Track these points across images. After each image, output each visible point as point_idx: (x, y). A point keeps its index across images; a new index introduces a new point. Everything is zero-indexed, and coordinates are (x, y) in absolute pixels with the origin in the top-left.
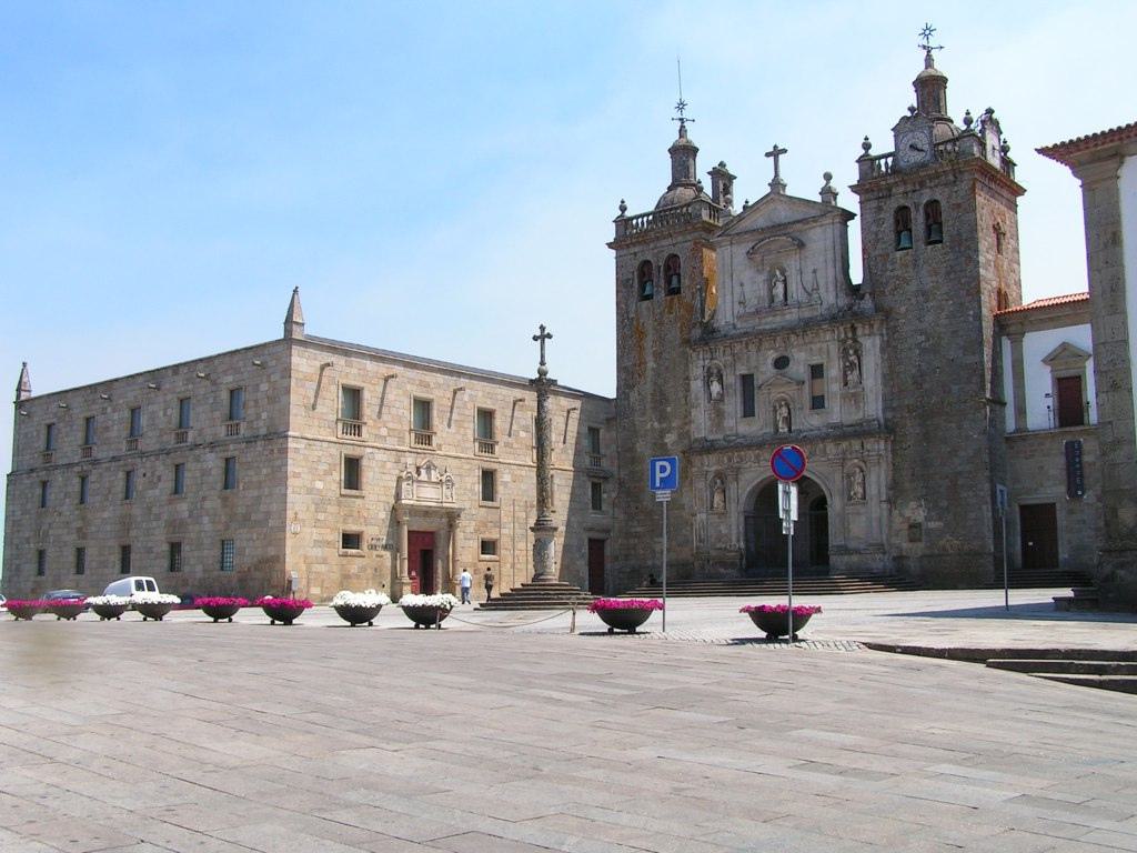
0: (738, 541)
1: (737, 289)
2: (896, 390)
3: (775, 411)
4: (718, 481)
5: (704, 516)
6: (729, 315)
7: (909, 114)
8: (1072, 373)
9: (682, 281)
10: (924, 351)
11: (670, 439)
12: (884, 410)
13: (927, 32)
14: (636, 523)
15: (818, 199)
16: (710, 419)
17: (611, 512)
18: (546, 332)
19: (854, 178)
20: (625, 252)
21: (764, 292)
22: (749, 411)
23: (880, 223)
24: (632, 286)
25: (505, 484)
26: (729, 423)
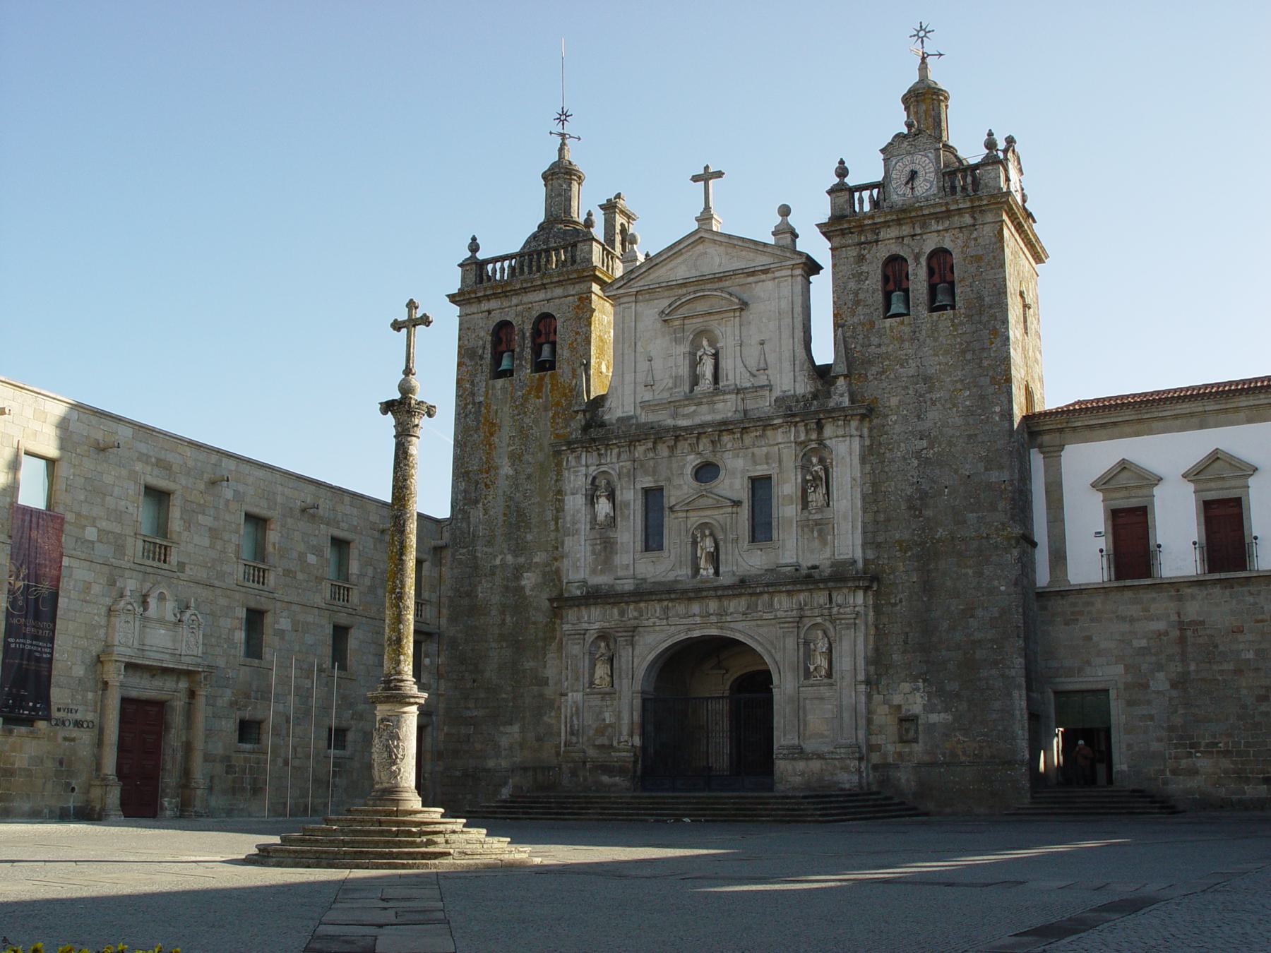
0: (631, 735)
1: (643, 366)
2: (882, 517)
3: (695, 543)
4: (603, 644)
5: (579, 696)
6: (629, 400)
7: (905, 131)
8: (1134, 503)
9: (559, 350)
11: (529, 580)
12: (865, 545)
13: (922, 34)
14: (471, 705)
15: (771, 240)
16: (593, 552)
17: (435, 686)
18: (418, 314)
19: (824, 214)
20: (474, 308)
21: (684, 370)
22: (652, 540)
23: (859, 277)
24: (481, 358)
25: (281, 634)
26: (622, 559)
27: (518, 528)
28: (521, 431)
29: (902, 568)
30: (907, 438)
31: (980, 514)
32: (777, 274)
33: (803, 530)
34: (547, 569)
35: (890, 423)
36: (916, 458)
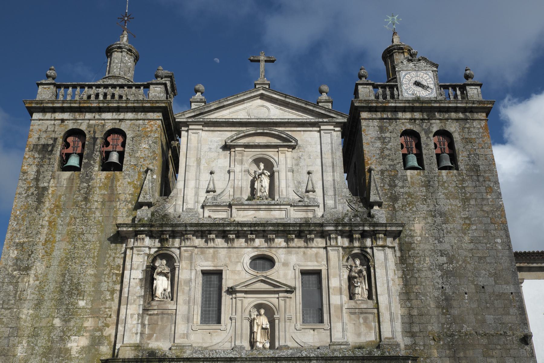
1: (205, 177)
3: (252, 322)
10: (447, 274)
26: (181, 328)
27: (70, 294)
28: (83, 214)
29: (436, 355)
30: (430, 255)
31: (497, 317)
32: (322, 127)
33: (350, 317)
34: (98, 334)
35: (416, 242)
36: (439, 269)
